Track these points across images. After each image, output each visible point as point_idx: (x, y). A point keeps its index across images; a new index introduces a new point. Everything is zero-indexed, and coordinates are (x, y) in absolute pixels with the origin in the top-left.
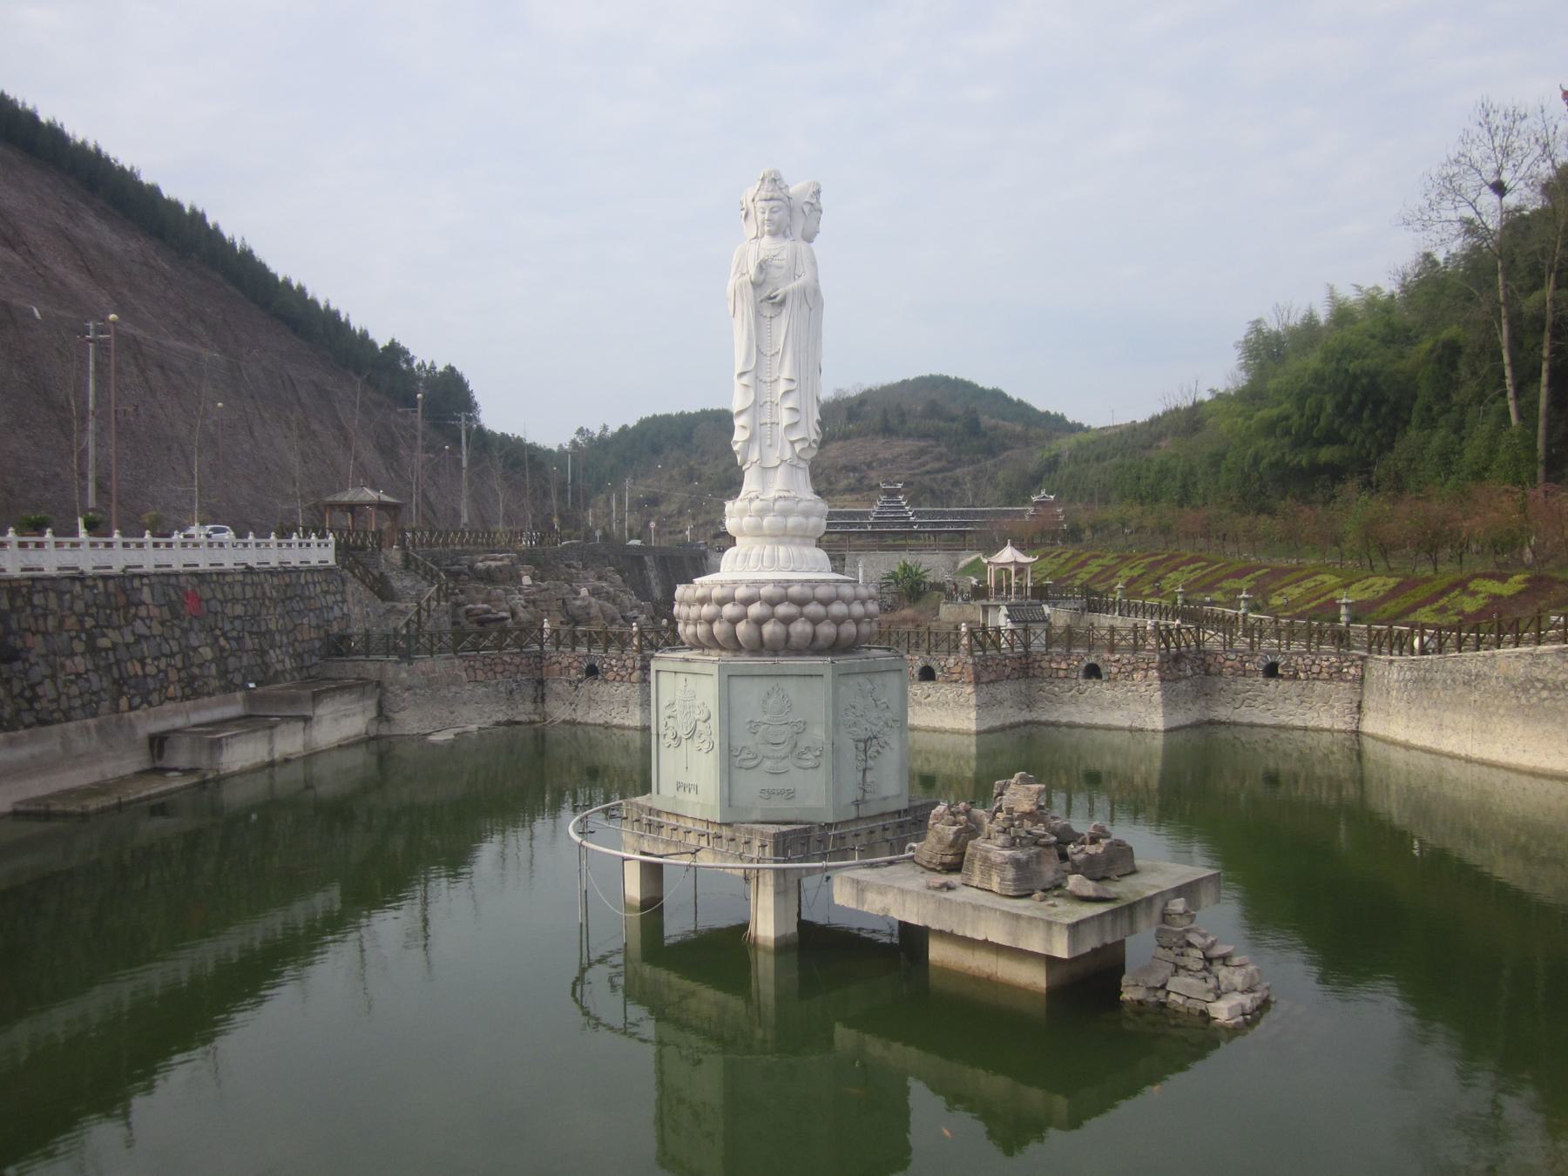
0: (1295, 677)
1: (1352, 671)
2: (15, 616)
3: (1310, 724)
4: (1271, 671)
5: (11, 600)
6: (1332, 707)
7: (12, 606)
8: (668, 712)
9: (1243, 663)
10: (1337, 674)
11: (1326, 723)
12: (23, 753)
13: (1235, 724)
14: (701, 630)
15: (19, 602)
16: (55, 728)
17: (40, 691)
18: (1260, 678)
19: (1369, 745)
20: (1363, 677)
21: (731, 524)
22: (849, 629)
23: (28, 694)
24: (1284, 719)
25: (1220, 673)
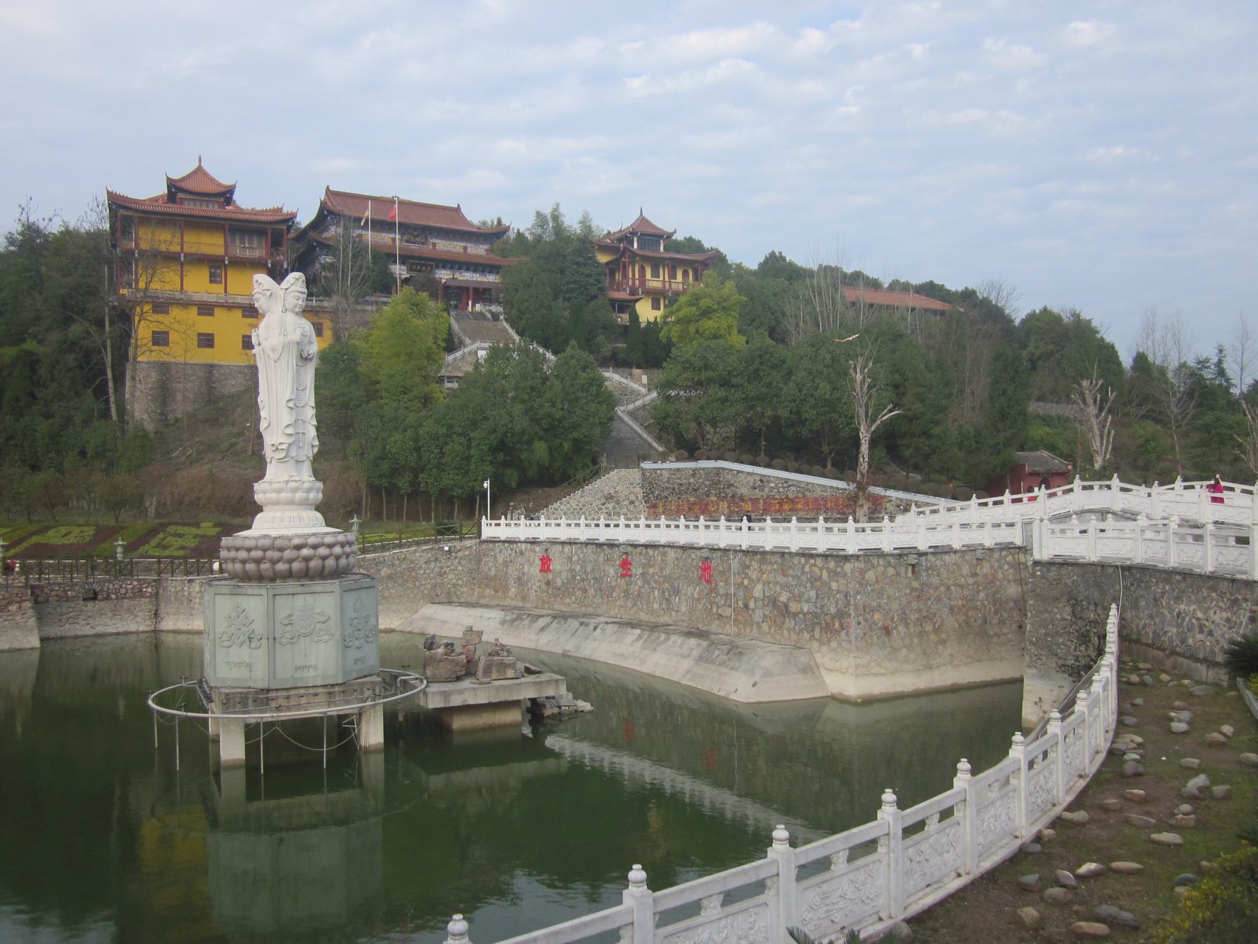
0: (108, 598)
1: (149, 590)
3: (121, 630)
4: (94, 597)
6: (136, 616)
8: (286, 621)
9: (66, 592)
10: (139, 593)
11: (133, 628)
13: (62, 638)
14: (303, 565)
18: (81, 602)
19: (164, 637)
20: (157, 593)
21: (258, 498)
22: (343, 561)
24: (100, 629)
25: (47, 601)
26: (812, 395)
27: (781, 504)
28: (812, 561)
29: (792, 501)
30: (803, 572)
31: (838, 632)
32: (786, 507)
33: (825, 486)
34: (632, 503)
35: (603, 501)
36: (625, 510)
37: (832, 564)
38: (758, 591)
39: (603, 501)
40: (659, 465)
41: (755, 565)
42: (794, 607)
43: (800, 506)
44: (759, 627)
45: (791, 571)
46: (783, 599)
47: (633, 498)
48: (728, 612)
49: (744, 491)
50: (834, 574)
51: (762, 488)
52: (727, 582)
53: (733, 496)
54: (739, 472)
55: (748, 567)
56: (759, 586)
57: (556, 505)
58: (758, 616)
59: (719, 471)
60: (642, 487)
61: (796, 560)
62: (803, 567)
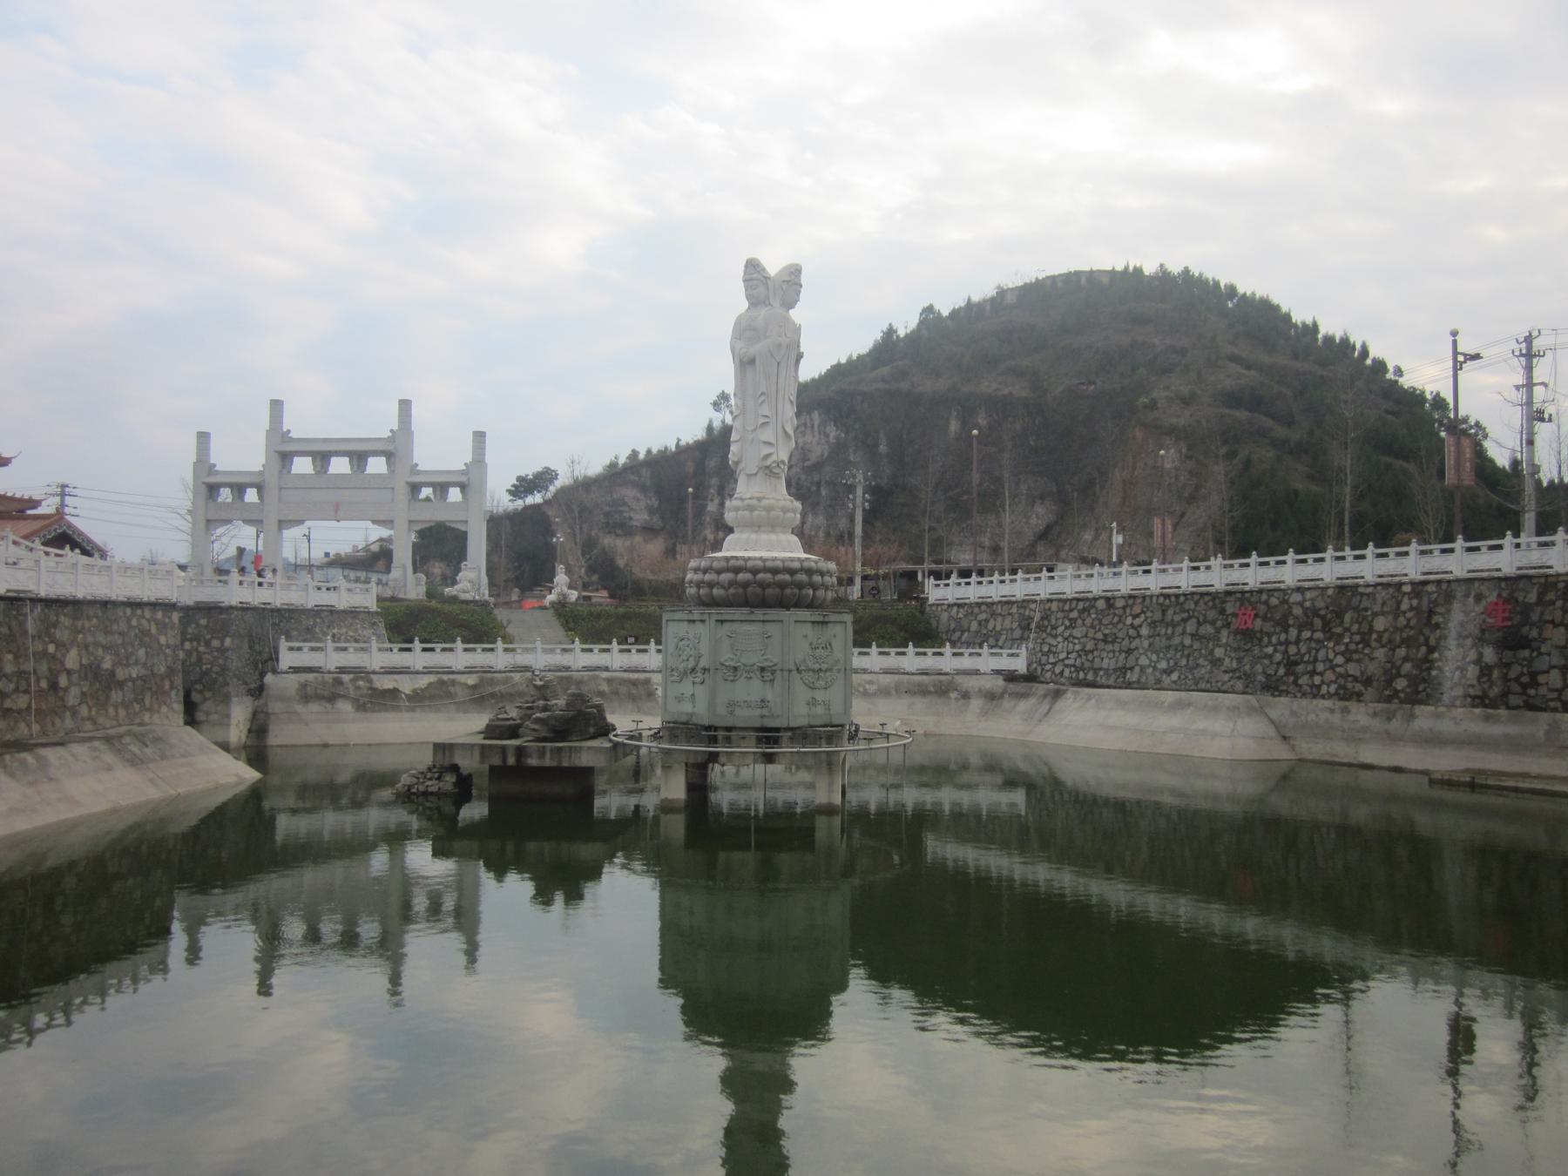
2: (1539, 609)
5: (1541, 595)
7: (1540, 602)
12: (1497, 730)
15: (1551, 596)
16: (1545, 717)
17: (1541, 679)
23: (1525, 679)
28: (139, 612)
30: (130, 627)
31: (165, 693)
37: (159, 615)
38: (72, 660)
41: (65, 621)
42: (121, 674)
44: (74, 714)
45: (115, 627)
46: (107, 665)
48: (22, 701)
50: (163, 627)
52: (16, 657)
55: (55, 625)
56: (73, 653)
58: (72, 698)
61: (120, 612)
62: (129, 620)
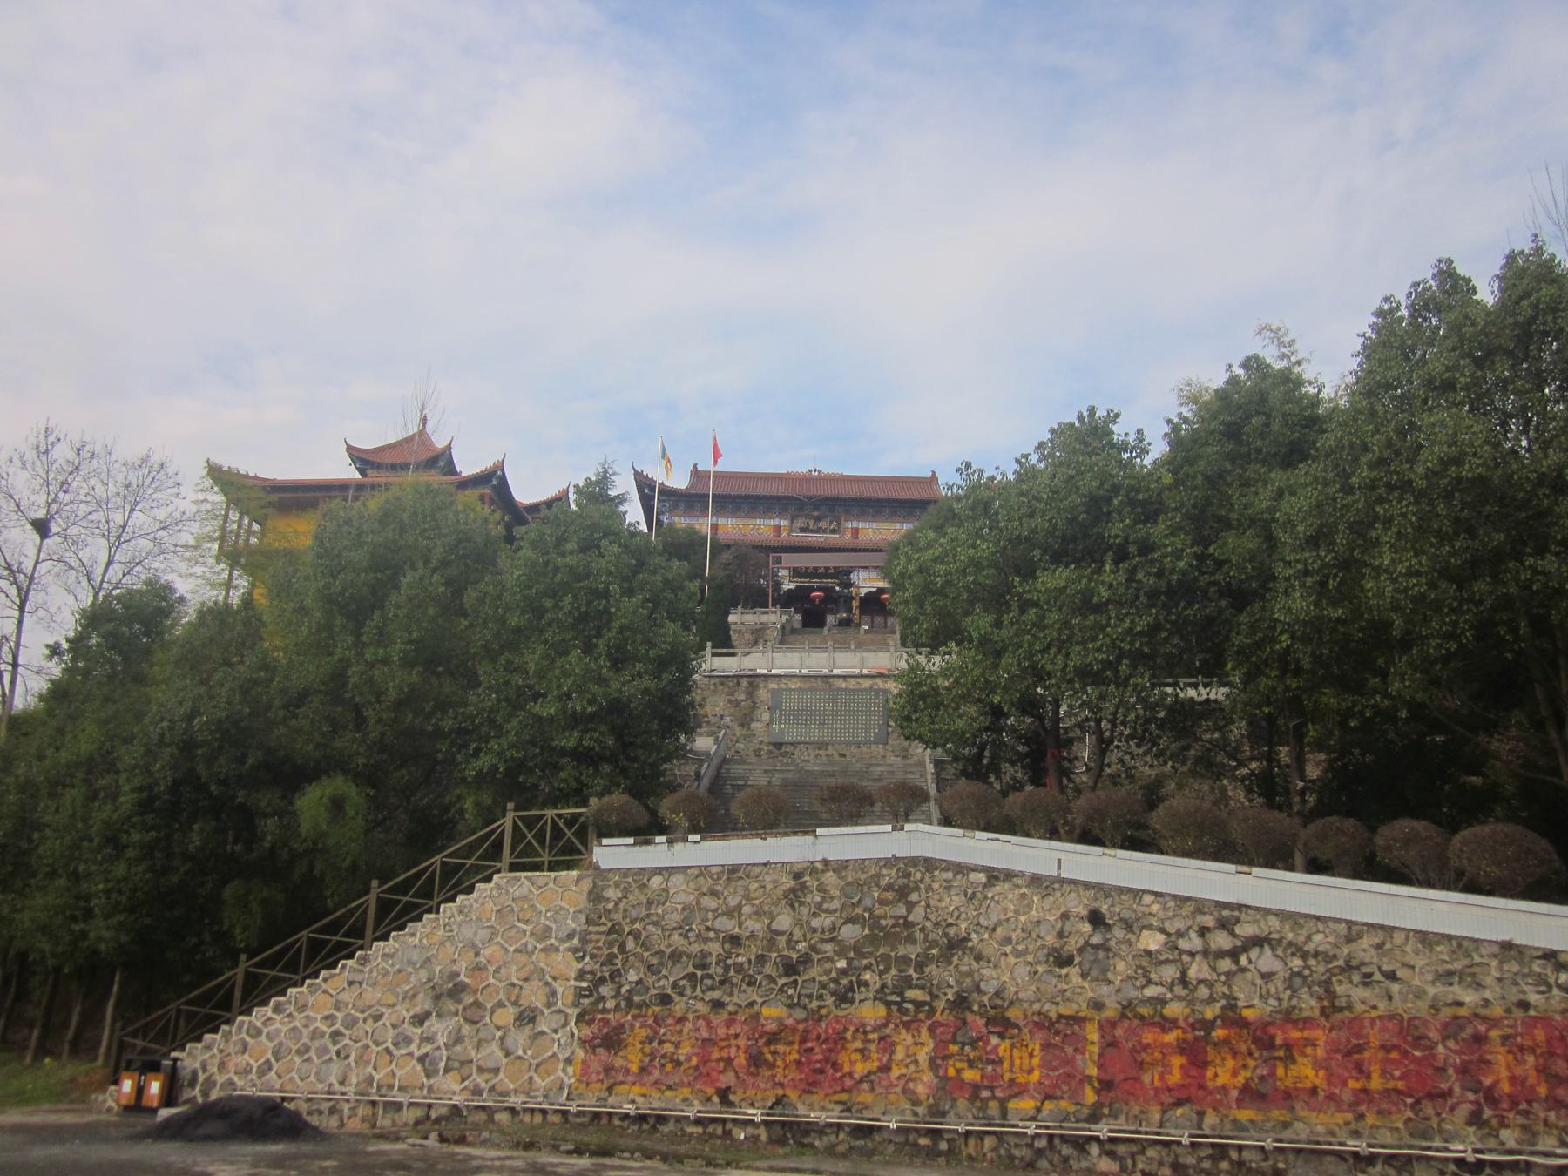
26: (1406, 486)
27: (1196, 1054)
29: (1263, 1041)
32: (1223, 1074)
33: (1460, 945)
34: (527, 1017)
35: (423, 1003)
36: (492, 1053)
39: (423, 1003)
40: (658, 853)
43: (1305, 1071)
47: (534, 996)
49: (1011, 975)
51: (1097, 958)
53: (961, 1003)
54: (994, 876)
57: (259, 1015)
59: (908, 876)
60: (579, 953)
